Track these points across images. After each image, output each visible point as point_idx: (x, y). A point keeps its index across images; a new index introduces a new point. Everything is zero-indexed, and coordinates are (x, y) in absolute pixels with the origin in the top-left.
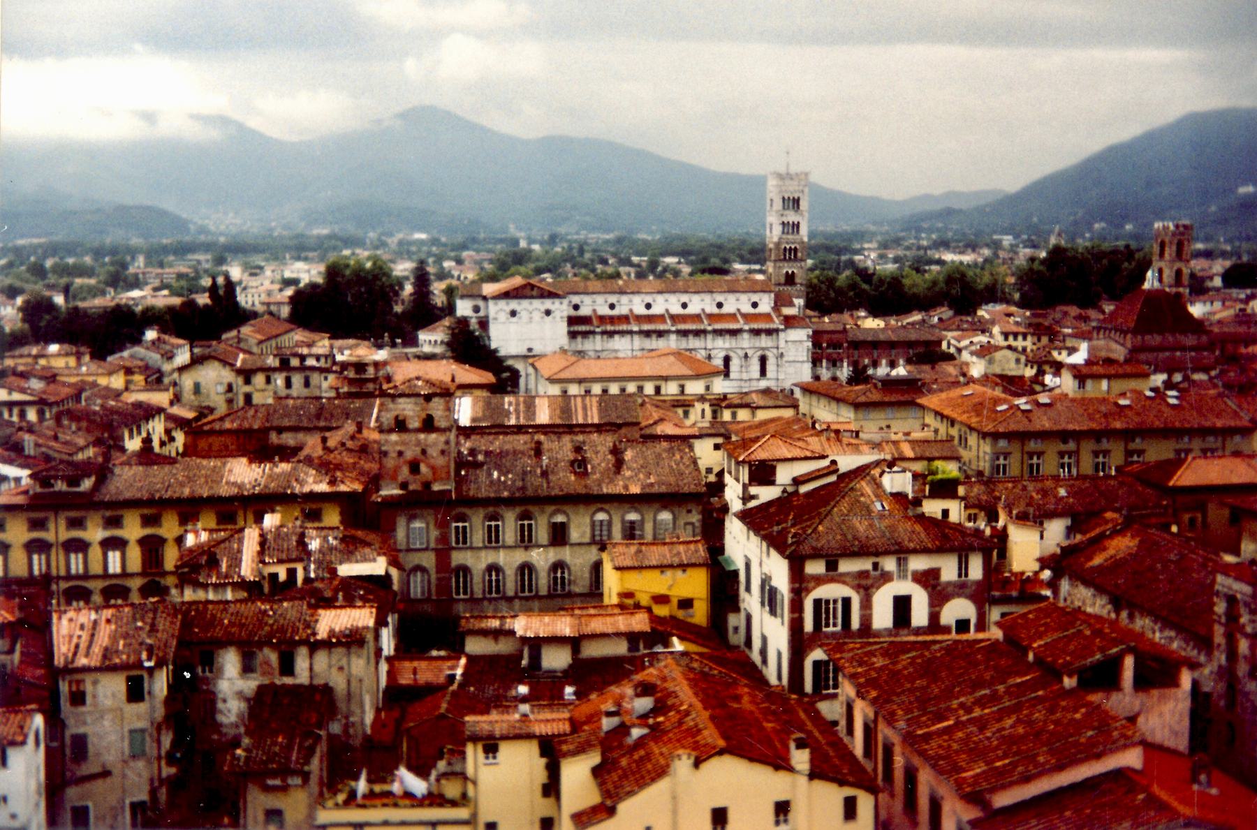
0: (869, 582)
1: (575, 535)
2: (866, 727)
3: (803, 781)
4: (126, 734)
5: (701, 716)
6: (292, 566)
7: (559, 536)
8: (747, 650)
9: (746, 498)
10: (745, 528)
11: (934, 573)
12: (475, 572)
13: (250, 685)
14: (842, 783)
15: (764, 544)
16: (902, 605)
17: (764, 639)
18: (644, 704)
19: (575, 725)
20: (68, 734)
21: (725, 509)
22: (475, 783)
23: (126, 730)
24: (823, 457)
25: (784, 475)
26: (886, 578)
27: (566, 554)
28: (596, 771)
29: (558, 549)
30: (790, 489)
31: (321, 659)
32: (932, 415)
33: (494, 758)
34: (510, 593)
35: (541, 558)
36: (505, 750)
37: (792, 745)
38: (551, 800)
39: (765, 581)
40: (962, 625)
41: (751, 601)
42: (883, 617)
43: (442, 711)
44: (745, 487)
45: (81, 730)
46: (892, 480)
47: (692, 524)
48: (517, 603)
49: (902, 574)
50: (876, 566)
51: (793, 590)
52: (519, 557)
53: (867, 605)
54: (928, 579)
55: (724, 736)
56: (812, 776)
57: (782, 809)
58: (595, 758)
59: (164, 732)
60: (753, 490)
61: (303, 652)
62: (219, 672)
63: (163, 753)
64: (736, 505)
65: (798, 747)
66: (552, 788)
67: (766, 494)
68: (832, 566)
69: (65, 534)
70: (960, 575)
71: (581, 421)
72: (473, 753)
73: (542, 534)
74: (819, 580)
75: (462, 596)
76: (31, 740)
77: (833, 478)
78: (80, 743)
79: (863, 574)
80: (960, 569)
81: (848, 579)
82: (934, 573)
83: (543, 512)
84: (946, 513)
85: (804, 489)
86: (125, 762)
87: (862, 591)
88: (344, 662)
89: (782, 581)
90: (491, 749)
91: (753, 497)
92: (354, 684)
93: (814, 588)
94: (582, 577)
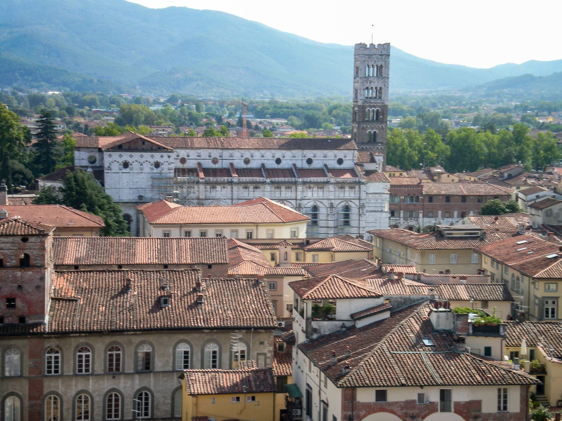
0: (416, 411)
1: (158, 364)
9: (308, 332)
10: (307, 360)
11: (478, 404)
12: (65, 398)
21: (291, 340)
24: (378, 296)
25: (344, 310)
27: (150, 381)
30: (348, 324)
32: (489, 260)
35: (128, 386)
44: (308, 321)
46: (438, 317)
47: (265, 354)
50: (421, 396)
52: (107, 384)
60: (314, 324)
64: (301, 339)
67: (325, 327)
70: (499, 408)
71: (176, 261)
77: (387, 315)
79: (409, 404)
81: (395, 409)
82: (478, 404)
83: (130, 342)
85: (360, 324)
91: (315, 331)
93: (365, 416)
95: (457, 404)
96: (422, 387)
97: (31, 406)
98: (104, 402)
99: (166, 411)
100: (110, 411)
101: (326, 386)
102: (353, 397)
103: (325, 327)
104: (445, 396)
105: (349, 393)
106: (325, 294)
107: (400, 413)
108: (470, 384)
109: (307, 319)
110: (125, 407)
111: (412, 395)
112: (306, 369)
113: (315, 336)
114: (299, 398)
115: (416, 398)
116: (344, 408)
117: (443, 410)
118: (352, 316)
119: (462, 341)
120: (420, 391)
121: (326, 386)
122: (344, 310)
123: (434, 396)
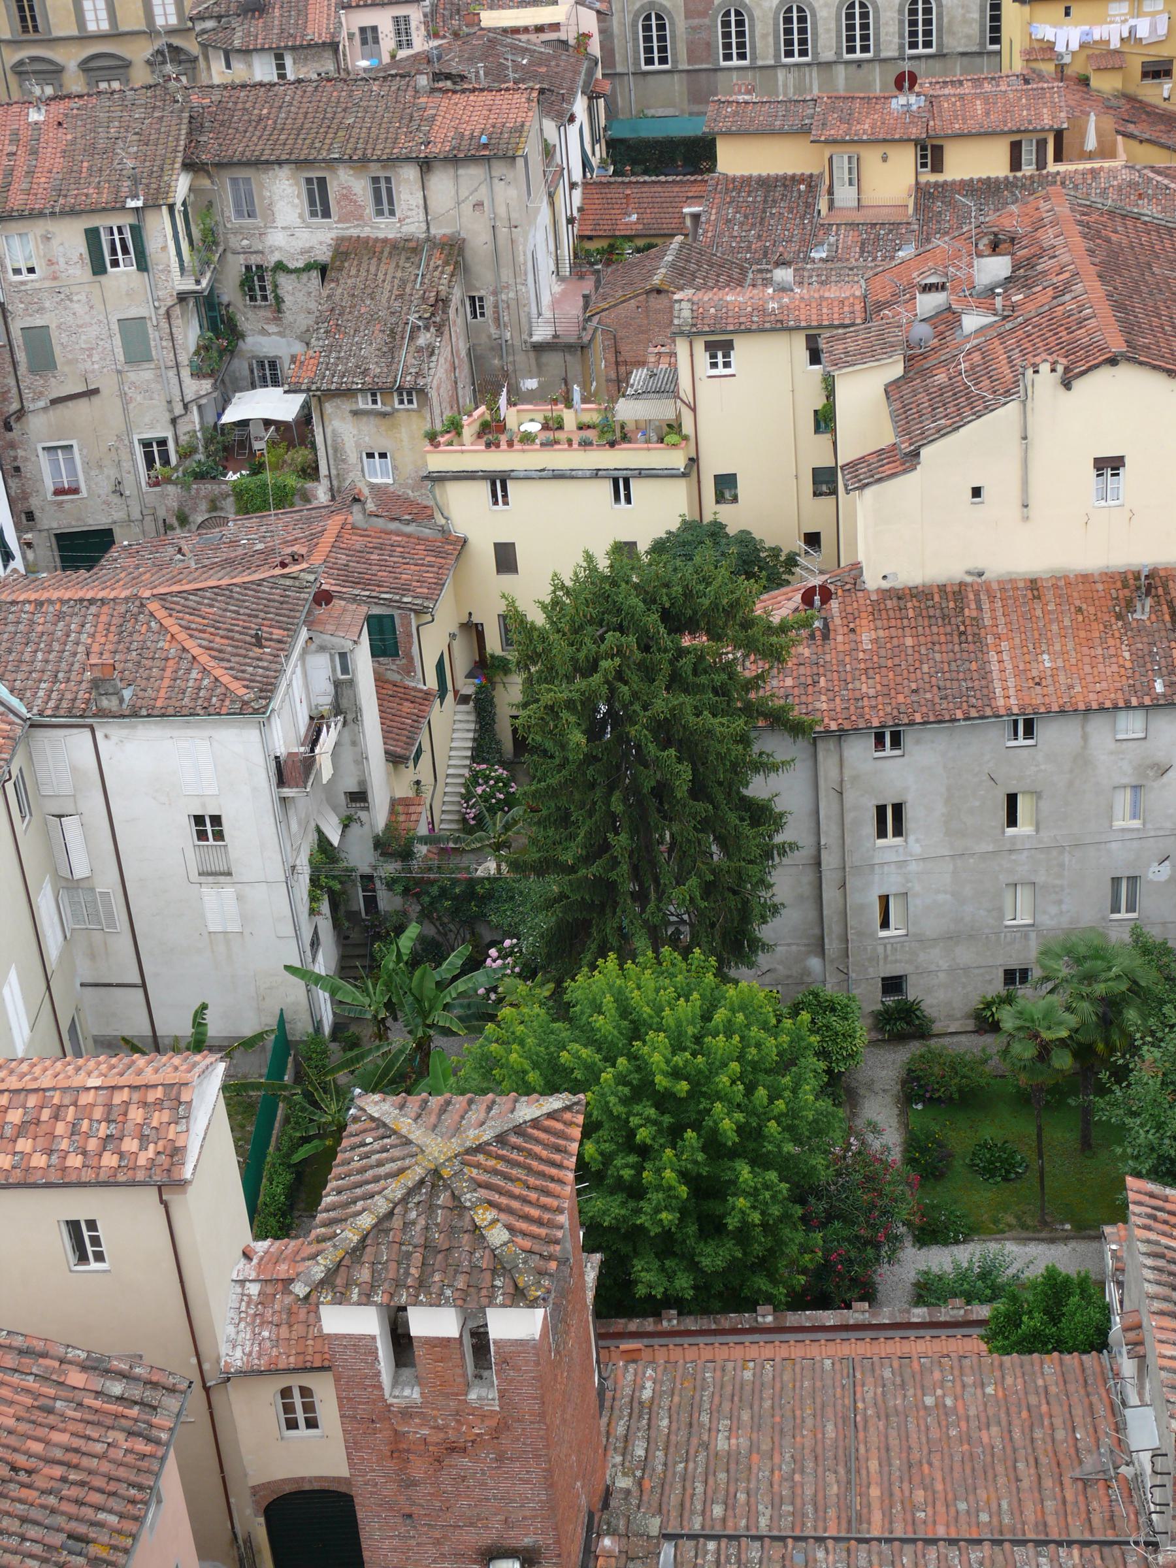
4: (115, 327)
5: (1090, 291)
6: (401, 11)
12: (757, 13)
18: (995, 268)
19: (872, 309)
20: (16, 327)
22: (694, 410)
23: (113, 320)
28: (891, 390)
31: (442, 183)
33: (727, 365)
34: (828, 55)
36: (745, 351)
38: (826, 438)
45: (38, 322)
48: (841, 70)
55: (1129, 329)
58: (896, 370)
59: (177, 322)
61: (410, 173)
62: (269, 214)
63: (184, 359)
66: (825, 420)
72: (690, 361)
75: (735, 62)
86: (119, 372)
88: (483, 194)
90: (720, 348)
92: (503, 232)
94: (965, 21)
97: (693, 29)
98: (838, 20)
99: (968, 37)
100: (851, 39)
110: (883, 31)
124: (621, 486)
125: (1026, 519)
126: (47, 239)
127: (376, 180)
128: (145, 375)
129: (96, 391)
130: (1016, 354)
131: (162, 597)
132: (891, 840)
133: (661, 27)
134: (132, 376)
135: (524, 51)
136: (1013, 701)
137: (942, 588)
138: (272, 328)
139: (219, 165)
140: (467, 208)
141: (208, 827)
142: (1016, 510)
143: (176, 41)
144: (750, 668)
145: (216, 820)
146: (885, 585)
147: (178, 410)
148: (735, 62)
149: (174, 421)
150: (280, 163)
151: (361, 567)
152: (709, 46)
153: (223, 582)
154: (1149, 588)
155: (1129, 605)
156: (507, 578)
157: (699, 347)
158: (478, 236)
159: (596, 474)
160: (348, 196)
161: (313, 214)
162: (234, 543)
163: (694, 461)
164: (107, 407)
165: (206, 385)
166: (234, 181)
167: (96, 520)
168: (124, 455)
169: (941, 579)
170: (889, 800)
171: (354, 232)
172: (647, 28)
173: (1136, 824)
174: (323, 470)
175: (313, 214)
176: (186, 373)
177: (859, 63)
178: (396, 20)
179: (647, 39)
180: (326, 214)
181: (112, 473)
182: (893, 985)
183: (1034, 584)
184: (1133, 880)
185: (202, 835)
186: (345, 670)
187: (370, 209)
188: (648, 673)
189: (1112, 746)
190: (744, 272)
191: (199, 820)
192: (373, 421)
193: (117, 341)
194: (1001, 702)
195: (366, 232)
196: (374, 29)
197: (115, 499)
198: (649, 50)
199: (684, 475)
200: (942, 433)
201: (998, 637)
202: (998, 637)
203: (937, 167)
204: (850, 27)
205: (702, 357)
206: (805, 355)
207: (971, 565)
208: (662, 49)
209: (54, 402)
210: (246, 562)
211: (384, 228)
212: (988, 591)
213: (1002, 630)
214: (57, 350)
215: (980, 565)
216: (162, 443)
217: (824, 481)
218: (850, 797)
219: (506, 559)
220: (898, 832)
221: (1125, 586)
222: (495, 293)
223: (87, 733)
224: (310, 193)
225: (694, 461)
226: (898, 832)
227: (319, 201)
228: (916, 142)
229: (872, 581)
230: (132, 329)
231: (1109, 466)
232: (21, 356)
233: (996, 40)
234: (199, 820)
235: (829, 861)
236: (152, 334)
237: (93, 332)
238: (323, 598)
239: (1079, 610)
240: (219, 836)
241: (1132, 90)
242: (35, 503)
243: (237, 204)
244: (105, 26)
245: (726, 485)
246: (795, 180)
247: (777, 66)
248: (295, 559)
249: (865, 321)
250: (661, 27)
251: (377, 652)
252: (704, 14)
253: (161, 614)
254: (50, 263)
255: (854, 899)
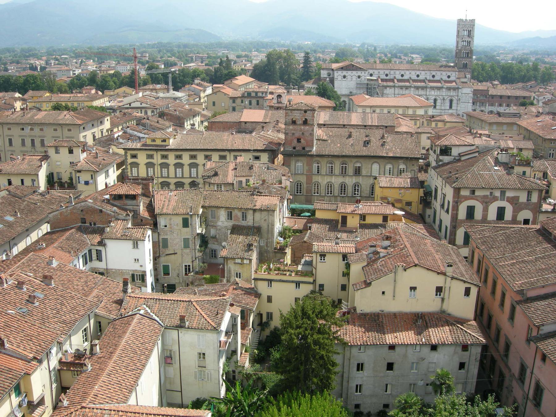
0: (488, 200)
1: (364, 172)
2: (479, 261)
3: (449, 279)
7: (358, 172)
8: (433, 225)
9: (437, 161)
10: (436, 174)
11: (517, 198)
13: (230, 224)
14: (465, 282)
15: (444, 181)
16: (501, 212)
17: (441, 221)
20: (161, 237)
21: (428, 165)
24: (473, 145)
26: (495, 199)
27: (360, 180)
29: (357, 177)
30: (457, 158)
31: (257, 215)
33: (324, 260)
34: (336, 195)
37: (446, 265)
38: (346, 278)
39: (445, 196)
40: (526, 222)
41: (437, 204)
42: (492, 215)
43: (305, 239)
45: (166, 237)
47: (414, 170)
49: (502, 199)
50: (491, 193)
51: (454, 202)
52: (340, 180)
53: (486, 210)
54: (513, 201)
56: (453, 278)
57: (439, 290)
59: (196, 240)
60: (441, 157)
61: (251, 212)
62: (218, 218)
64: (434, 164)
65: (448, 266)
66: (346, 274)
68: (473, 192)
69: (161, 161)
70: (528, 200)
71: (370, 124)
73: (350, 171)
74: (467, 198)
75: (316, 194)
76: (147, 239)
77: (477, 154)
78: (165, 241)
79: (485, 197)
80: (528, 197)
81: (479, 199)
82: (517, 198)
83: (351, 161)
84: (524, 173)
87: (484, 204)
88: (266, 217)
89: (450, 197)
91: (441, 161)
92: (270, 226)
95: (508, 198)
96: (492, 189)
101: (445, 186)
102: (459, 192)
103: (446, 159)
104: (503, 193)
105: (457, 191)
106: (447, 143)
107: (480, 200)
108: (515, 189)
109: (437, 155)
111: (487, 193)
112: (435, 179)
113: (440, 163)
114: (431, 192)
115: (489, 194)
116: (454, 197)
117: (501, 200)
118: (459, 154)
119: (513, 168)
120: (491, 191)
121: (445, 186)
122: (455, 152)
123: (497, 194)
124: (298, 284)
125: (394, 299)
126: (170, 219)
127: (243, 213)
128: (187, 251)
129: (176, 253)
130: (392, 262)
131: (196, 301)
132: (360, 372)
133: (301, 186)
134: (185, 251)
135: (275, 188)
136: (391, 341)
137: (374, 314)
138: (216, 243)
139: (209, 207)
140: (263, 220)
141: (202, 355)
142: (392, 297)
143: (195, 180)
144: (334, 329)
145: (204, 354)
146: (361, 312)
147: (194, 259)
148: (316, 194)
149: (193, 262)
150: (222, 207)
151: (238, 299)
152: (311, 191)
153: (210, 299)
154: (421, 317)
155: (417, 321)
156: (269, 304)
157: (318, 256)
158: (264, 226)
159: (293, 282)
160: (236, 216)
161: (228, 219)
162: (206, 290)
163: (314, 281)
164: (178, 258)
165: (201, 254)
166: (212, 211)
167: (172, 282)
168: (181, 268)
169: (374, 312)
170: (360, 362)
171: (237, 224)
172: (297, 186)
173: (416, 371)
174: (226, 276)
175: (228, 219)
176: (197, 251)
177: (343, 197)
178: (246, 180)
179: (297, 188)
180: (231, 219)
181: (177, 271)
182: (357, 406)
183: (395, 315)
184: (414, 384)
185: (200, 358)
186: (235, 321)
187: (241, 219)
188: (312, 329)
189: (412, 353)
190: (323, 239)
191: (200, 354)
192: (239, 265)
193: (182, 243)
194: (388, 341)
195: (240, 224)
196: (241, 181)
197: (177, 277)
198: (297, 190)
199: (313, 283)
200: (377, 279)
201: (387, 326)
202: (387, 326)
203: (364, 220)
204: (342, 189)
205: (319, 258)
206: (341, 258)
207: (381, 309)
208: (300, 190)
209: (167, 255)
210: (210, 294)
211: (244, 223)
212: (385, 316)
213: (388, 324)
214: (169, 243)
215: (383, 309)
216: (189, 266)
217: (344, 287)
218: (352, 360)
219: (269, 299)
220: (362, 370)
221: (415, 316)
222: (267, 240)
223: (177, 331)
224: (228, 214)
225: (314, 281)
226: (362, 370)
227: (230, 216)
228: (360, 214)
229: (358, 311)
230: (186, 241)
231: (413, 289)
232: (161, 244)
233: (372, 195)
234: (200, 354)
235: (345, 375)
236: (190, 242)
237: (177, 240)
238: (232, 305)
239: (405, 321)
240: (204, 358)
241: (403, 207)
242: (159, 277)
243: (212, 215)
244: (181, 176)
245: (322, 286)
246: (332, 220)
247: (325, 196)
248: (224, 295)
249: (356, 252)
250: (301, 186)
251: (242, 318)
252: (310, 184)
253: (196, 305)
254: (170, 225)
255: (350, 385)
